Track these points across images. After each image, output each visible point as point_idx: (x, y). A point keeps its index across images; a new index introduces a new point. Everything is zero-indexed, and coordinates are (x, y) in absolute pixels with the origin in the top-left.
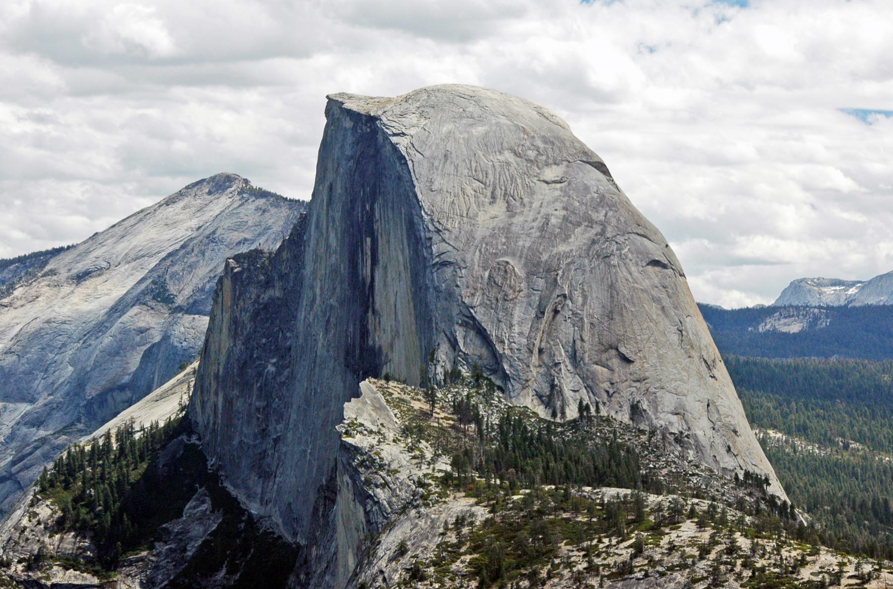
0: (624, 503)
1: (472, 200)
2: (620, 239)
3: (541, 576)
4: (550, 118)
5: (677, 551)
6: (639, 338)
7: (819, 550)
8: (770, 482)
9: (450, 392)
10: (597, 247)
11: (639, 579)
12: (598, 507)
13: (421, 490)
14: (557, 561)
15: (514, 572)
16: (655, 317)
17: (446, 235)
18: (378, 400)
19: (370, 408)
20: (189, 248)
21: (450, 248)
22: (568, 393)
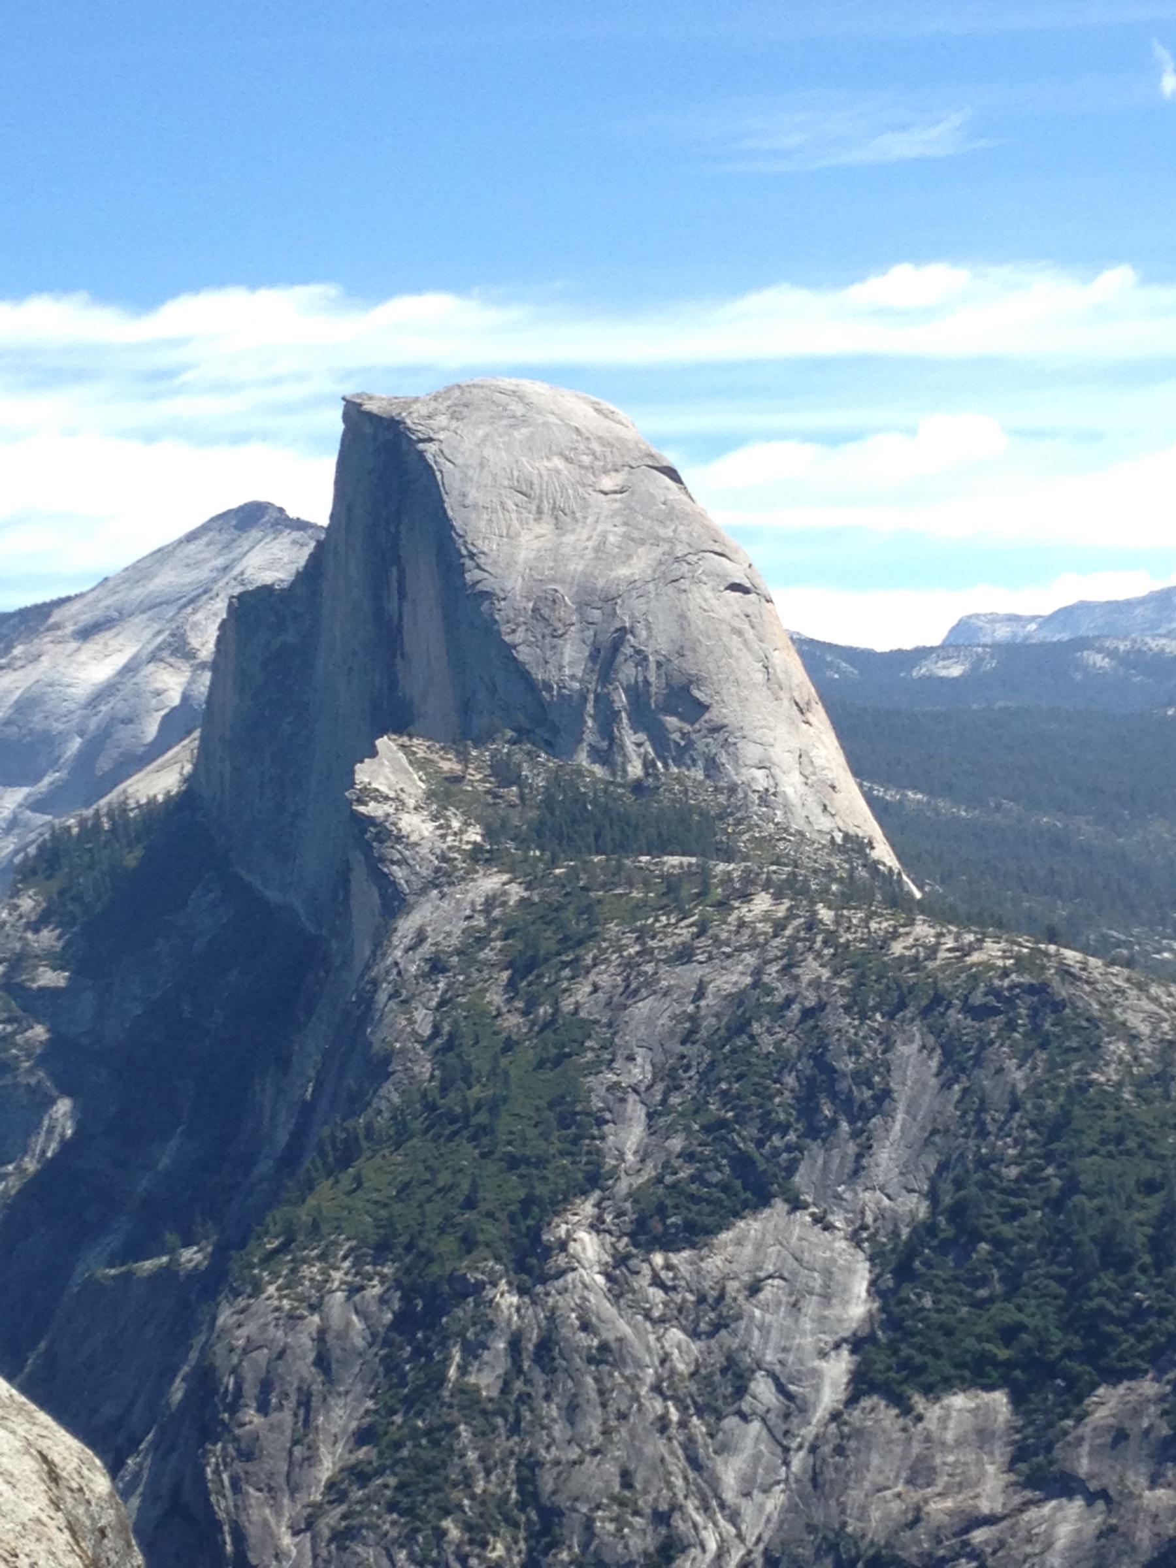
0: (688, 873)
1: (514, 516)
2: (695, 558)
3: (584, 963)
4: (610, 415)
5: (747, 927)
6: (715, 678)
7: (914, 920)
8: (875, 845)
9: (487, 750)
10: (663, 568)
11: (701, 963)
12: (658, 880)
13: (444, 865)
14: (604, 945)
15: (555, 960)
16: (734, 651)
17: (482, 560)
18: (399, 760)
19: (387, 771)
20: (213, 593)
21: (486, 575)
22: (630, 748)
